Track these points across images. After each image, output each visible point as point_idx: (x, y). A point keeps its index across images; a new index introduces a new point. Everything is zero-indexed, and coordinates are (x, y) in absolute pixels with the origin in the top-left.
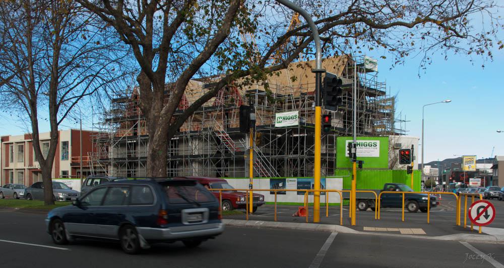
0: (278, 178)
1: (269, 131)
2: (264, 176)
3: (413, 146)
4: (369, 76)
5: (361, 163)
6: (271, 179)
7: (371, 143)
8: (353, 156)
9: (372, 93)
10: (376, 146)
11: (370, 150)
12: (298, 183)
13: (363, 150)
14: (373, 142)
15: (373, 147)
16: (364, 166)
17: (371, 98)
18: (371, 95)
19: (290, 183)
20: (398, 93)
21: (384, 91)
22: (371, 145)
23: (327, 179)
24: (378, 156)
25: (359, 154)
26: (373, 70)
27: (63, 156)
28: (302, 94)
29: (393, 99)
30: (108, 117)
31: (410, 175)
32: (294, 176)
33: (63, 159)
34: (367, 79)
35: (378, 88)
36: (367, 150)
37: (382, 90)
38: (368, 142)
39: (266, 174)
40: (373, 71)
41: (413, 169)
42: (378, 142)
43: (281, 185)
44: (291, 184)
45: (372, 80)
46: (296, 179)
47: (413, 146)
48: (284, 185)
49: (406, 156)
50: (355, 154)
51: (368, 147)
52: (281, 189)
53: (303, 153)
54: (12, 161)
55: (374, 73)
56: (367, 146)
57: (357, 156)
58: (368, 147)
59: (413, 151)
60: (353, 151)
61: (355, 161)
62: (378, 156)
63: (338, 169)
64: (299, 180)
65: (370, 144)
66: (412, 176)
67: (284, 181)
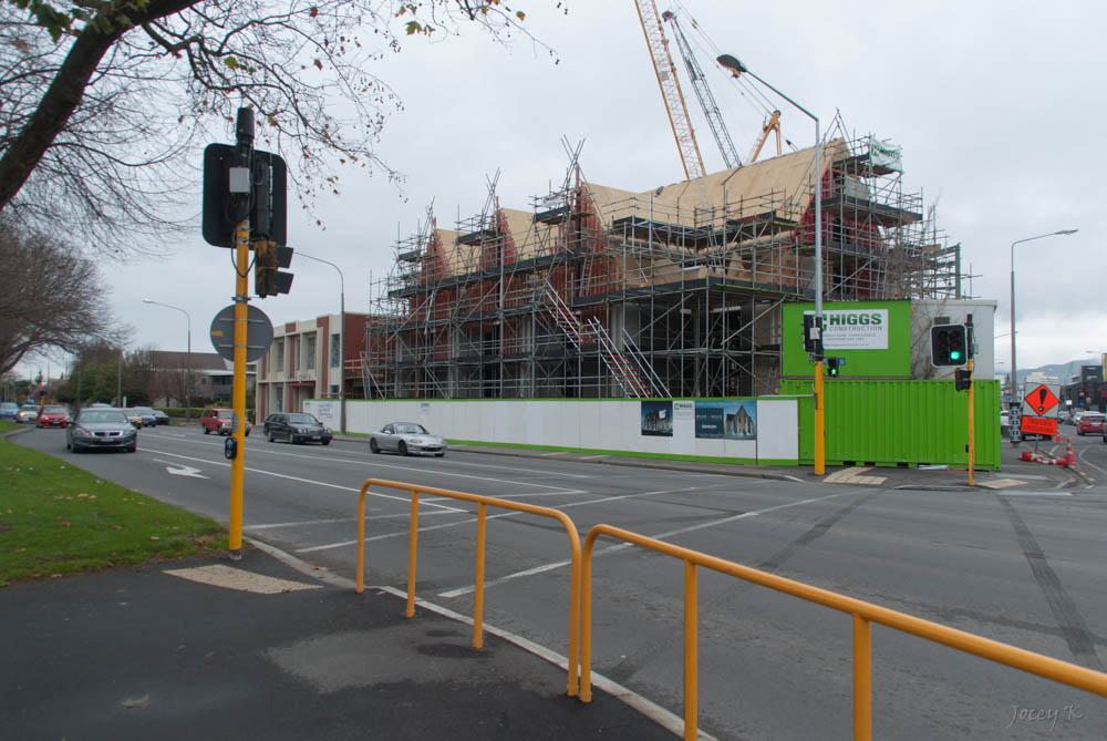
0: (656, 399)
1: (649, 300)
2: (634, 396)
3: (970, 317)
4: (881, 181)
5: (833, 363)
6: (643, 403)
7: (867, 316)
8: (814, 347)
9: (894, 217)
10: (880, 322)
11: (858, 332)
12: (698, 411)
13: (847, 333)
14: (870, 312)
15: (870, 325)
16: (844, 370)
17: (892, 230)
18: (888, 223)
19: (682, 410)
20: (937, 199)
21: (920, 212)
22: (867, 321)
23: (758, 402)
24: (886, 347)
25: (831, 342)
26: (891, 167)
27: (333, 360)
28: (730, 222)
29: (956, 249)
30: (393, 289)
31: (963, 392)
32: (685, 396)
33: (333, 366)
34: (882, 191)
35: (905, 206)
36: (856, 332)
37: (914, 210)
38: (858, 313)
39: (639, 391)
40: (891, 172)
41: (973, 377)
42: (884, 314)
43: (662, 414)
44: (683, 415)
45: (889, 188)
46: (691, 402)
47: (970, 317)
48: (669, 416)
49: (951, 340)
50: (819, 342)
51: (859, 324)
52: (660, 426)
53: (717, 345)
54: (298, 368)
55: (896, 174)
56: (855, 322)
57: (825, 347)
58: (859, 324)
59: (970, 332)
60: (814, 333)
61: (820, 359)
62: (886, 347)
63: (791, 378)
64: (701, 405)
65: (864, 318)
66: (972, 396)
67: (668, 406)
